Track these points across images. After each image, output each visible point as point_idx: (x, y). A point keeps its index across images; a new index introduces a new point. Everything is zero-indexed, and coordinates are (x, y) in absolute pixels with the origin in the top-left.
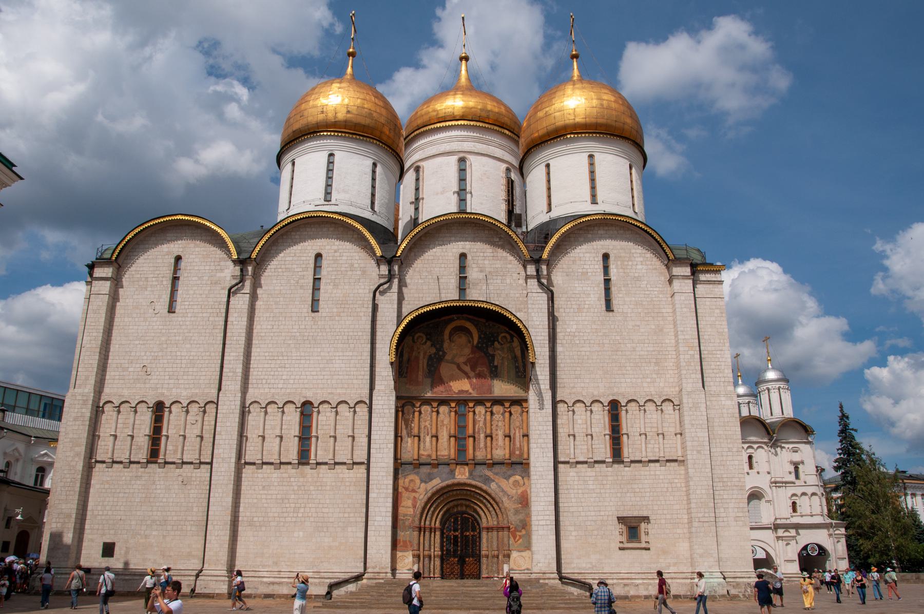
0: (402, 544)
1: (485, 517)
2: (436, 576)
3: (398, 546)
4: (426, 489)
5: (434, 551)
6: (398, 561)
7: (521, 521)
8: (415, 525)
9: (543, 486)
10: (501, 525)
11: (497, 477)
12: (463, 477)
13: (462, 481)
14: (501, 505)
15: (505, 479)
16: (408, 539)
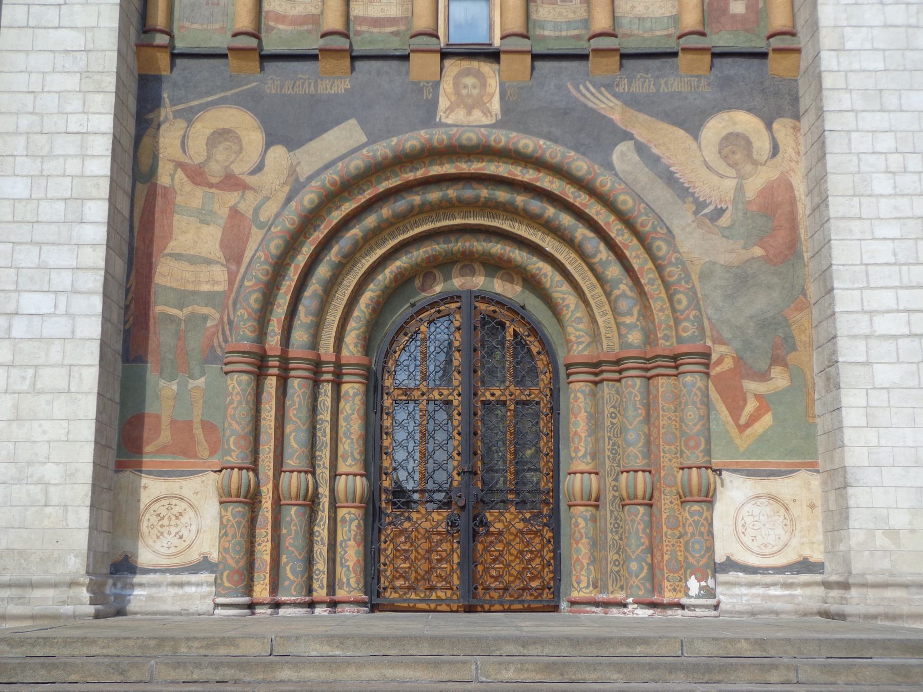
0: (165, 436)
1: (581, 313)
2: (341, 594)
3: (147, 449)
4: (292, 171)
5: (334, 475)
6: (144, 525)
7: (765, 324)
8: (233, 344)
9: (886, 143)
10: (666, 345)
11: (642, 117)
12: (477, 117)
13: (470, 137)
14: (661, 246)
15: (681, 125)
16: (197, 415)
